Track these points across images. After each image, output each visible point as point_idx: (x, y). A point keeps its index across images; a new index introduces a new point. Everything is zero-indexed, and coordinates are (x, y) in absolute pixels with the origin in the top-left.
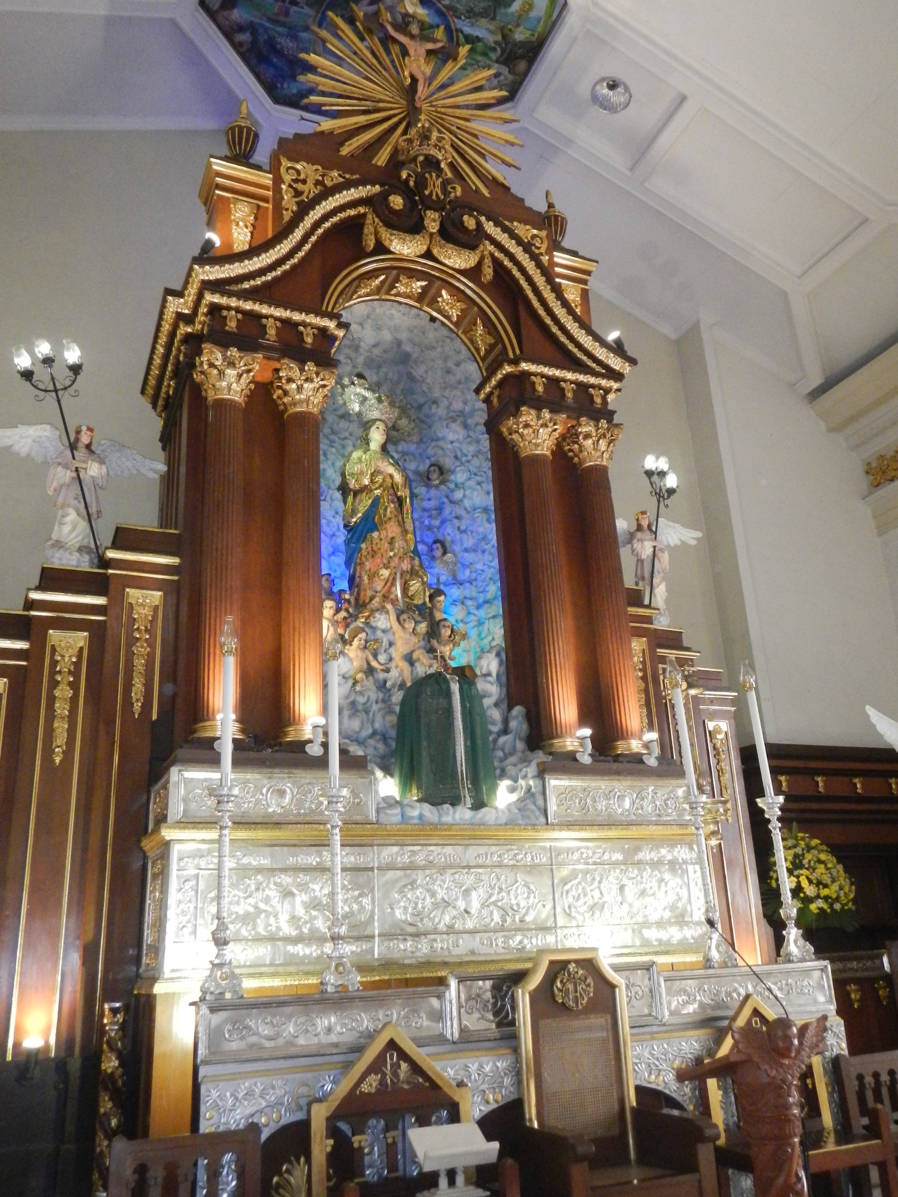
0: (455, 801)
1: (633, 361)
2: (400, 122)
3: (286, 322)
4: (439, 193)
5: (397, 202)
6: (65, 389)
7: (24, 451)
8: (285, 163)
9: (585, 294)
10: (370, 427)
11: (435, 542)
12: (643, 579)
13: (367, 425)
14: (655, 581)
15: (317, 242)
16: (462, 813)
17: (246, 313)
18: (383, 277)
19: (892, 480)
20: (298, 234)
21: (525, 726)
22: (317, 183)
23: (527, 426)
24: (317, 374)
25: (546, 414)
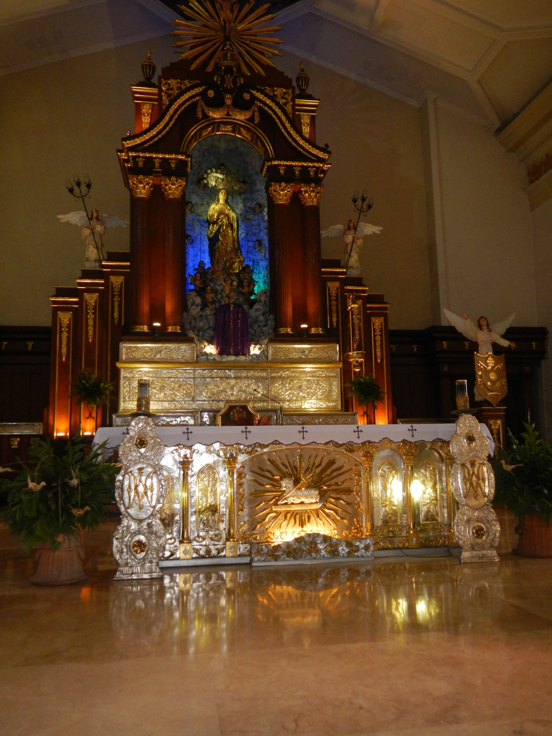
0: (229, 354)
1: (329, 153)
2: (220, 44)
3: (163, 159)
4: (231, 85)
5: (211, 93)
6: (86, 195)
7: (74, 223)
8: (163, 81)
9: (313, 118)
10: (219, 192)
11: (256, 241)
12: (347, 253)
13: (219, 191)
14: (352, 254)
15: (177, 118)
16: (232, 358)
17: (146, 158)
18: (212, 127)
19: (537, 179)
20: (167, 118)
21: (273, 323)
22: (179, 88)
23: (275, 191)
24: (177, 181)
25: (283, 184)
